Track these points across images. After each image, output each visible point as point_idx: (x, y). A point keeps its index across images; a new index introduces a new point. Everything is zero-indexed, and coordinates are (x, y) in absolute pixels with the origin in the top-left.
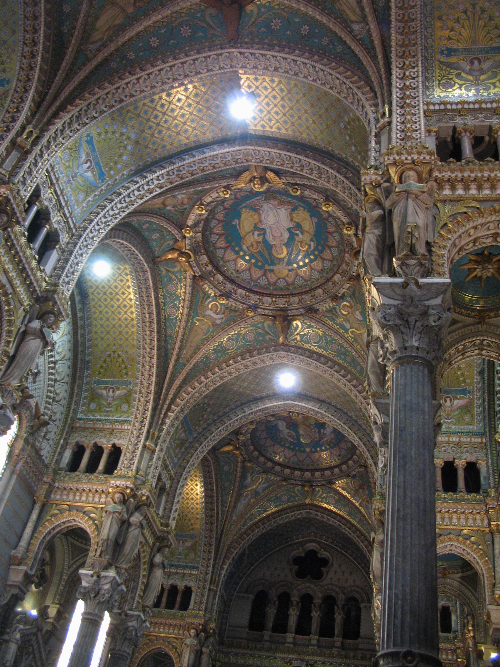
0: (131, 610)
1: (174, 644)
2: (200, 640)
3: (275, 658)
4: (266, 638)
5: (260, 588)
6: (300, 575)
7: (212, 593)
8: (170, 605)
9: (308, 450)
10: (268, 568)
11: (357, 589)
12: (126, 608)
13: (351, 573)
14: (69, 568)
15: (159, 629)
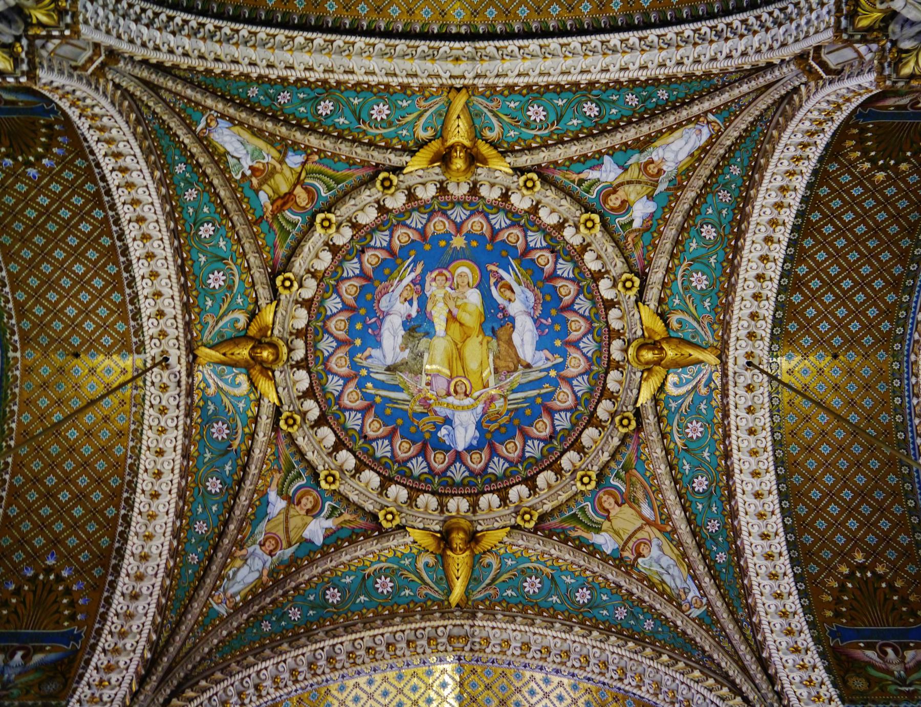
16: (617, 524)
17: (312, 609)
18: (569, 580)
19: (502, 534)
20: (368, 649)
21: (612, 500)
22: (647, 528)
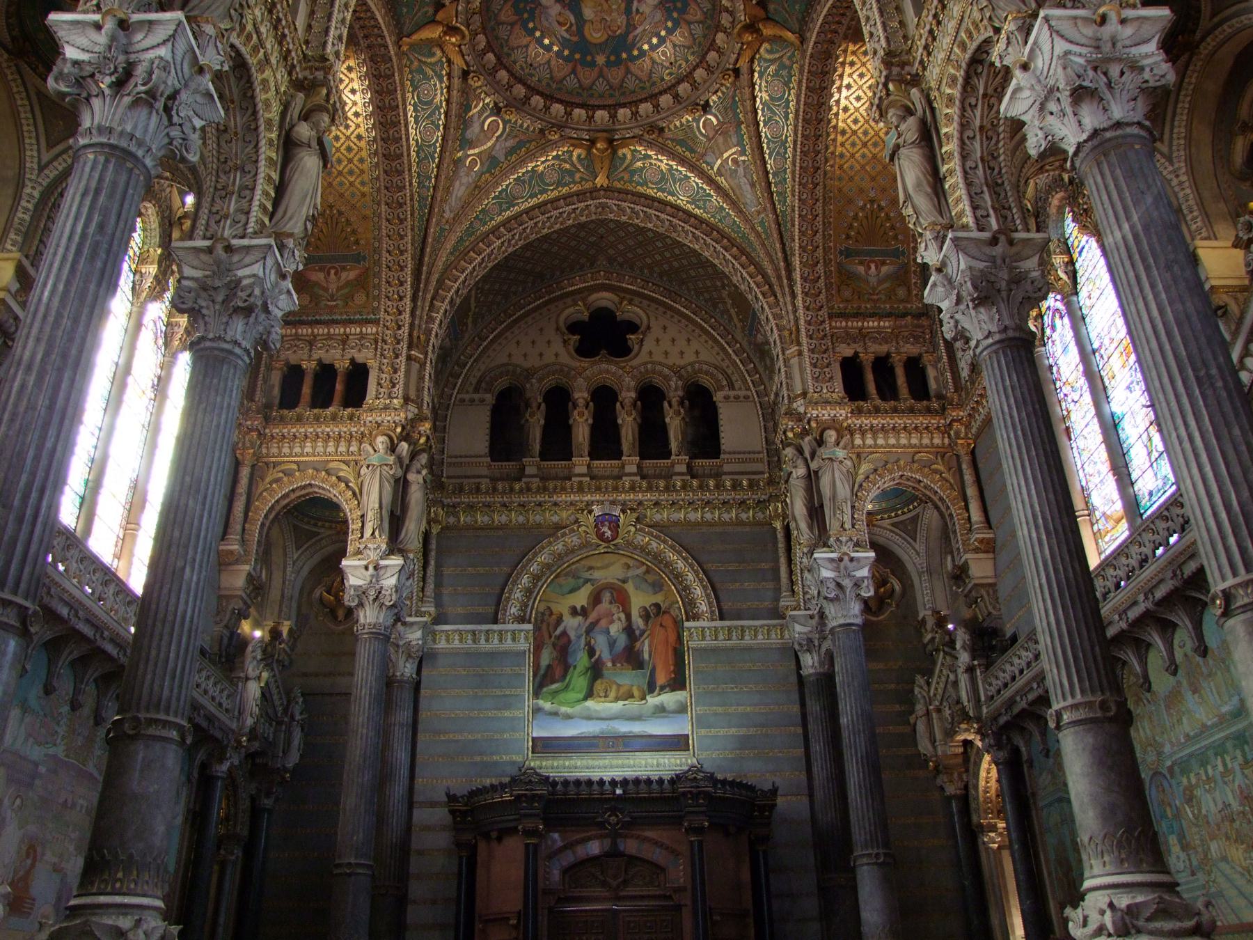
0: (243, 237)
1: (341, 474)
2: (400, 459)
3: (555, 504)
4: (530, 470)
5: (502, 384)
6: (584, 351)
7: (416, 366)
8: (322, 399)
9: (601, 60)
10: (518, 343)
11: (705, 367)
12: (227, 233)
13: (689, 340)
14: (41, 169)
15: (302, 448)
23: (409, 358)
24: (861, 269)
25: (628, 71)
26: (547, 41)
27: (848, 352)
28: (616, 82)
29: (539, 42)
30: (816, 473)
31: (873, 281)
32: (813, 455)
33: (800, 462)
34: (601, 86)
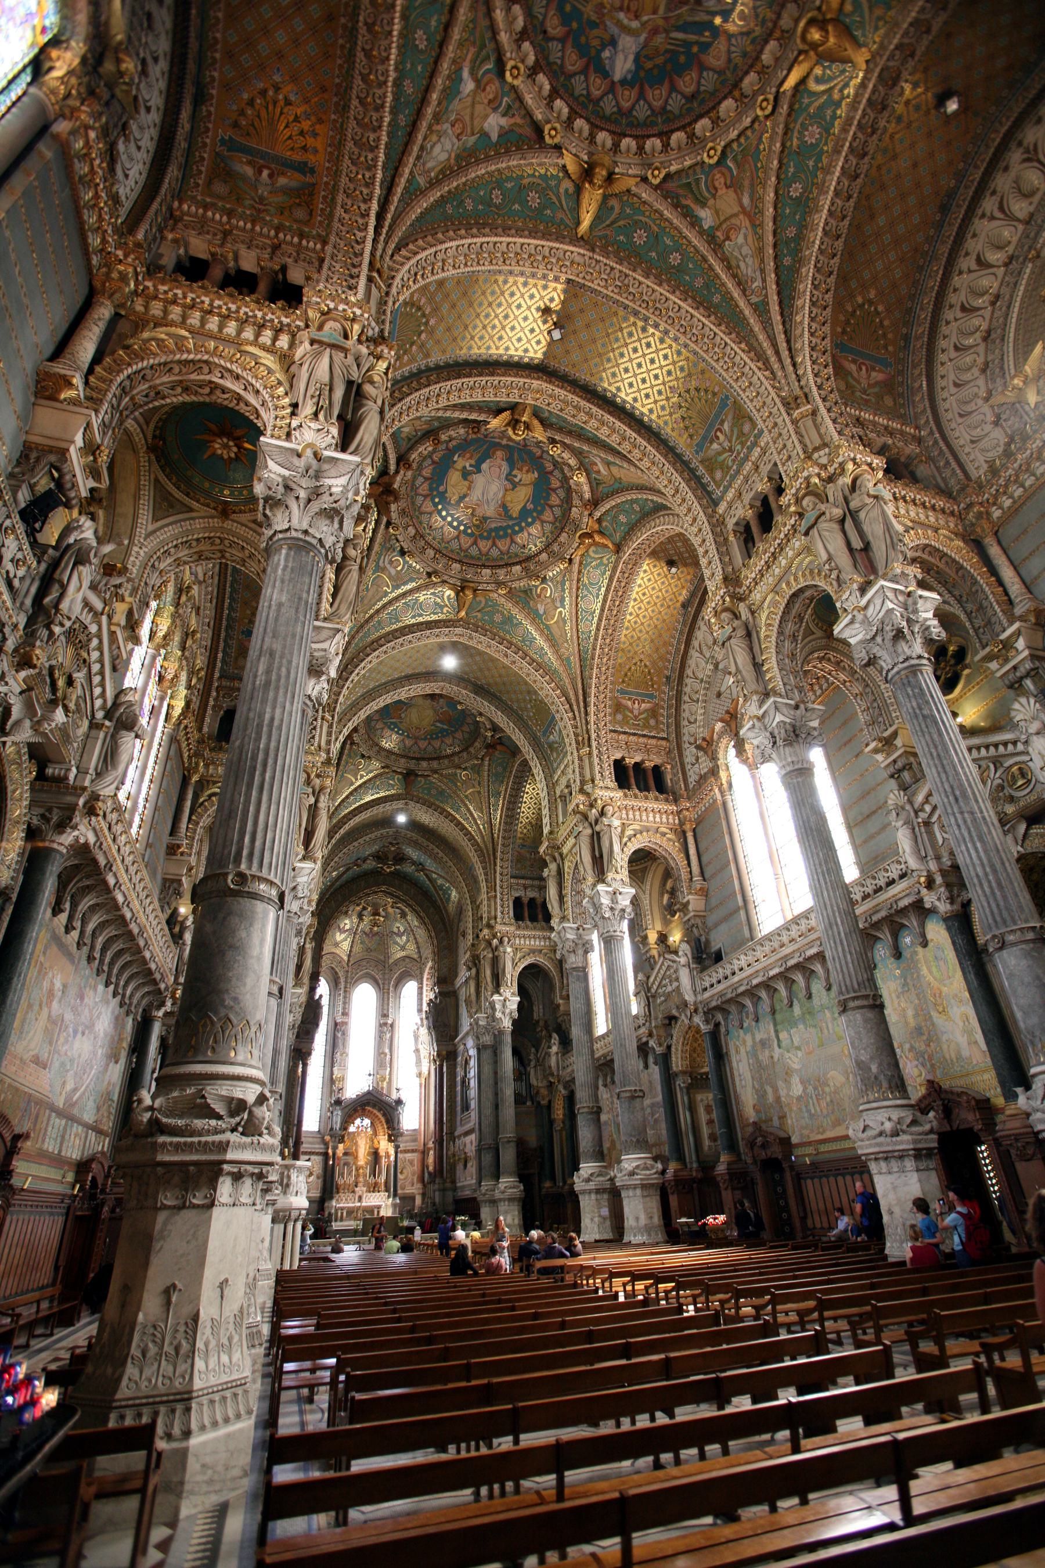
16: (720, 204)
17: (481, 203)
18: (668, 242)
19: (632, 182)
20: (517, 254)
21: (722, 180)
22: (741, 217)
23: (323, 718)
24: (629, 703)
25: (494, 544)
26: (444, 513)
27: (618, 756)
28: (484, 550)
29: (439, 512)
30: (598, 833)
31: (636, 712)
32: (596, 822)
33: (586, 824)
34: (474, 551)
